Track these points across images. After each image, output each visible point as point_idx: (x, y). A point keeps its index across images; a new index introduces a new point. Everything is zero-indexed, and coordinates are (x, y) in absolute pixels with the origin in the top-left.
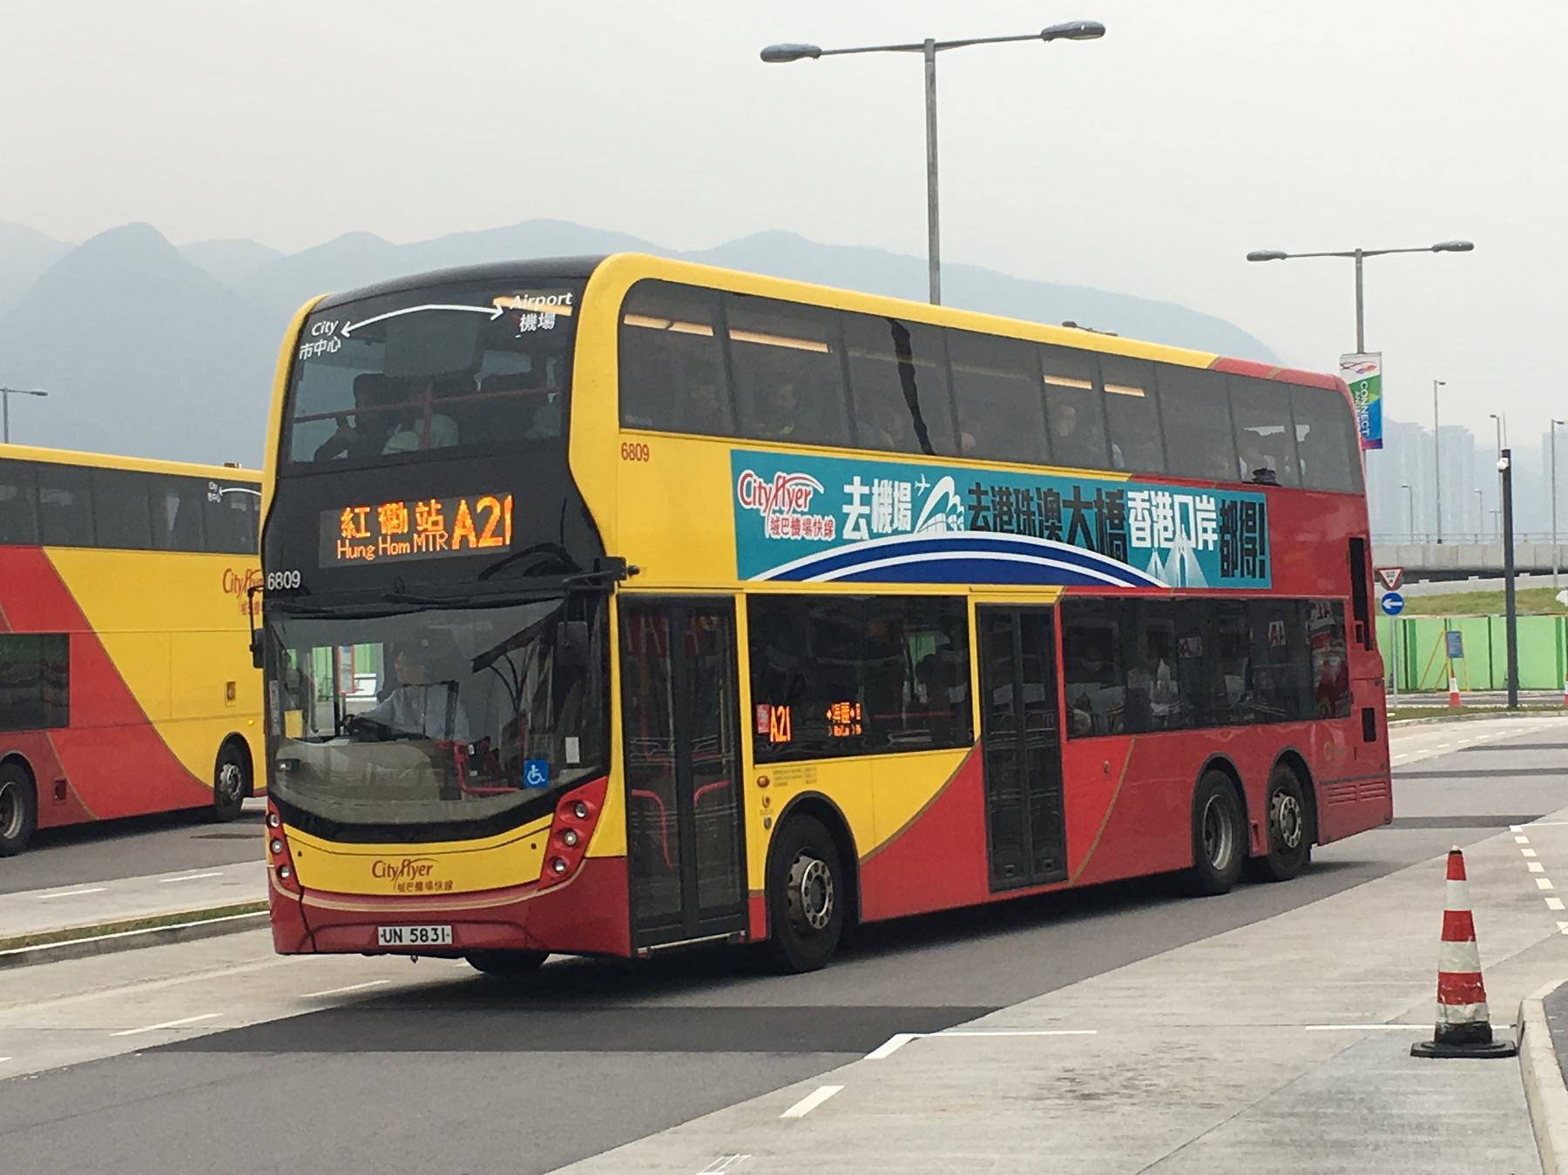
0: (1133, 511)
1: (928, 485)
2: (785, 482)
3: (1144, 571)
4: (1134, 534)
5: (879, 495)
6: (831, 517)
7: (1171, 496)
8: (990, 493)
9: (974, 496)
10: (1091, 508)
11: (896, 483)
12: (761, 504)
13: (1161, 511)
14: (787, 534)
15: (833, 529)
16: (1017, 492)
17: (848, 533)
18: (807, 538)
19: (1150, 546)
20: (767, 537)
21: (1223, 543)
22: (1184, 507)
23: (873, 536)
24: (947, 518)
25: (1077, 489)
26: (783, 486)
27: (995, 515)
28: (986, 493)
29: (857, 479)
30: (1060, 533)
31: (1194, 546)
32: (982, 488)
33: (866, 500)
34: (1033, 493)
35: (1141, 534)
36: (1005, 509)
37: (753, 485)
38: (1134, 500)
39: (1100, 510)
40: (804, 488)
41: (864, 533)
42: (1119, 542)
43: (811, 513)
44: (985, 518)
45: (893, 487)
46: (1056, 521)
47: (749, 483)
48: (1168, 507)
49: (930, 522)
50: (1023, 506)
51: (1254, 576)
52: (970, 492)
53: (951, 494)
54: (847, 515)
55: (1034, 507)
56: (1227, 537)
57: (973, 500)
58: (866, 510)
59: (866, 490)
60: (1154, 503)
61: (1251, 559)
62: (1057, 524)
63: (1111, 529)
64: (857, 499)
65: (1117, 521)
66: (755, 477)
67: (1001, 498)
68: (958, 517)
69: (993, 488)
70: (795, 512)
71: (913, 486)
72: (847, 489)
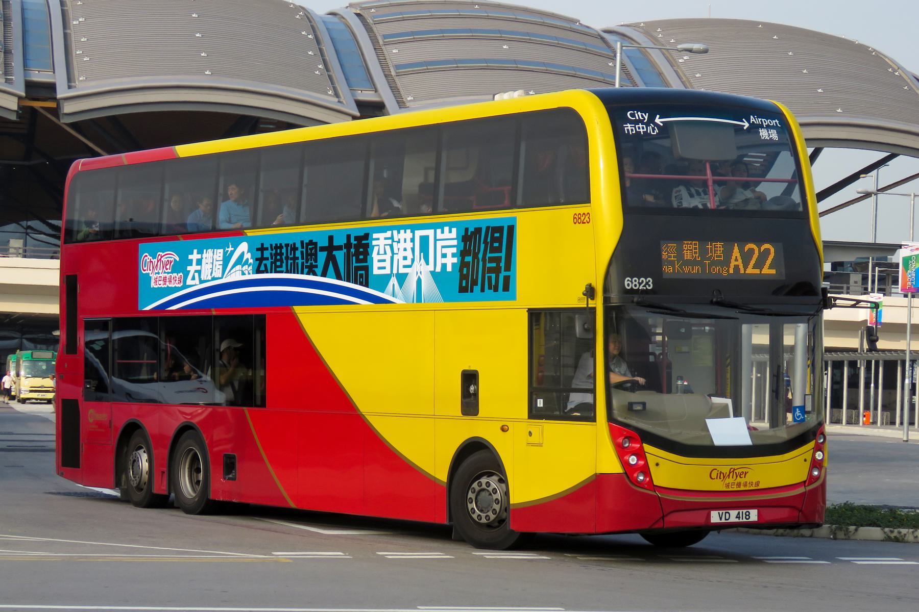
0: (376, 249)
1: (233, 249)
2: (162, 257)
3: (383, 292)
4: (376, 265)
5: (206, 258)
6: (181, 274)
7: (413, 232)
8: (269, 249)
9: (260, 252)
10: (342, 250)
11: (215, 250)
12: (150, 270)
13: (402, 245)
14: (160, 285)
15: (182, 280)
16: (287, 245)
17: (189, 282)
18: (170, 286)
19: (389, 272)
20: (152, 287)
21: (463, 264)
22: (424, 240)
23: (201, 282)
24: (242, 268)
25: (331, 238)
26: (160, 259)
27: (271, 262)
28: (267, 249)
29: (195, 251)
30: (315, 269)
31: (433, 270)
32: (265, 246)
33: (199, 262)
34: (298, 245)
35: (382, 264)
36: (278, 257)
37: (148, 260)
38: (378, 239)
39: (349, 251)
40: (169, 259)
41: (197, 281)
42: (363, 272)
43: (172, 273)
44: (265, 265)
45: (213, 253)
46: (313, 262)
47: (146, 260)
48: (408, 240)
49: (232, 271)
50: (291, 254)
51: (496, 290)
52: (258, 249)
53: (246, 253)
54: (190, 271)
55: (298, 254)
56: (468, 259)
57: (259, 254)
58: (198, 268)
59: (199, 256)
60: (396, 239)
61: (493, 276)
62: (314, 264)
63: (356, 263)
64: (194, 262)
65: (361, 257)
66: (148, 257)
67: (276, 251)
68: (249, 266)
69: (271, 245)
70: (165, 273)
71: (224, 251)
72: (190, 257)
